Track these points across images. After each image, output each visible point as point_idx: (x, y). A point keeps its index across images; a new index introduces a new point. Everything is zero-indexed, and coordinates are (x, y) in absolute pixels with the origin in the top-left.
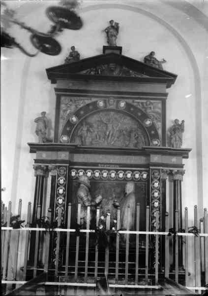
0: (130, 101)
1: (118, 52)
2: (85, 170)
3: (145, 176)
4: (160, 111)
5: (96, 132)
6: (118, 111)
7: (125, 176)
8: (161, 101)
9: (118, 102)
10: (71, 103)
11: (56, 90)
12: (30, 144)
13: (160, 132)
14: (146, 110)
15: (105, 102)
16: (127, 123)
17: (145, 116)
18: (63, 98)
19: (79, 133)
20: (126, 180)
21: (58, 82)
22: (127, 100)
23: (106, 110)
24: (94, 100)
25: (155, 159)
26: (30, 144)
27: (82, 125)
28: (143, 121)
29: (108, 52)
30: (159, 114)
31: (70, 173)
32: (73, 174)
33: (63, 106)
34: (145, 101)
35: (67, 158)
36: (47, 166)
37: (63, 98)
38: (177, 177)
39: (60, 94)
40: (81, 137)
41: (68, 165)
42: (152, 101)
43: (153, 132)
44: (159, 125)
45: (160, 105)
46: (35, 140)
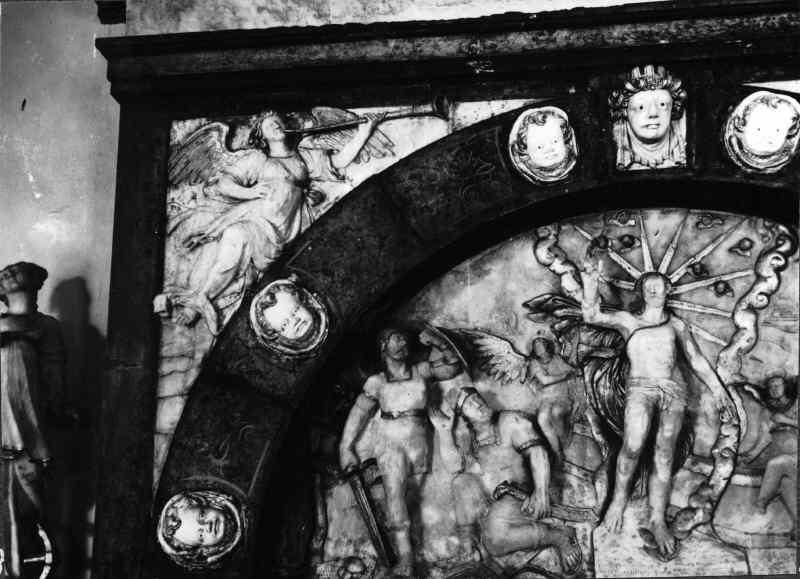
5: (516, 429)
23: (601, 190)
40: (365, 474)
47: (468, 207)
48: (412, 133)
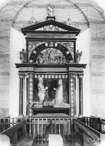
0: (60, 43)
1: (53, 19)
2: (41, 75)
3: (67, 77)
4: (73, 47)
6: (54, 47)
7: (58, 77)
8: (73, 42)
9: (54, 44)
10: (33, 45)
11: (26, 38)
12: (16, 64)
13: (73, 57)
14: (67, 47)
15: (48, 43)
16: (59, 53)
17: (66, 50)
18: (29, 42)
19: (38, 58)
20: (58, 79)
21: (27, 34)
22: (58, 42)
23: (49, 47)
24: (43, 43)
25: (71, 69)
26: (16, 64)
27: (39, 55)
28: (65, 52)
29: (49, 19)
30: (73, 48)
31: (34, 76)
32: (36, 77)
33: (30, 46)
34: (66, 42)
35: (32, 70)
36: (24, 74)
37: (29, 42)
38: (81, 77)
39: (28, 40)
41: (33, 73)
42: (69, 43)
43: (70, 57)
44: (72, 53)
45: (73, 44)
46: (20, 62)
47: (43, 47)
48: (41, 43)
